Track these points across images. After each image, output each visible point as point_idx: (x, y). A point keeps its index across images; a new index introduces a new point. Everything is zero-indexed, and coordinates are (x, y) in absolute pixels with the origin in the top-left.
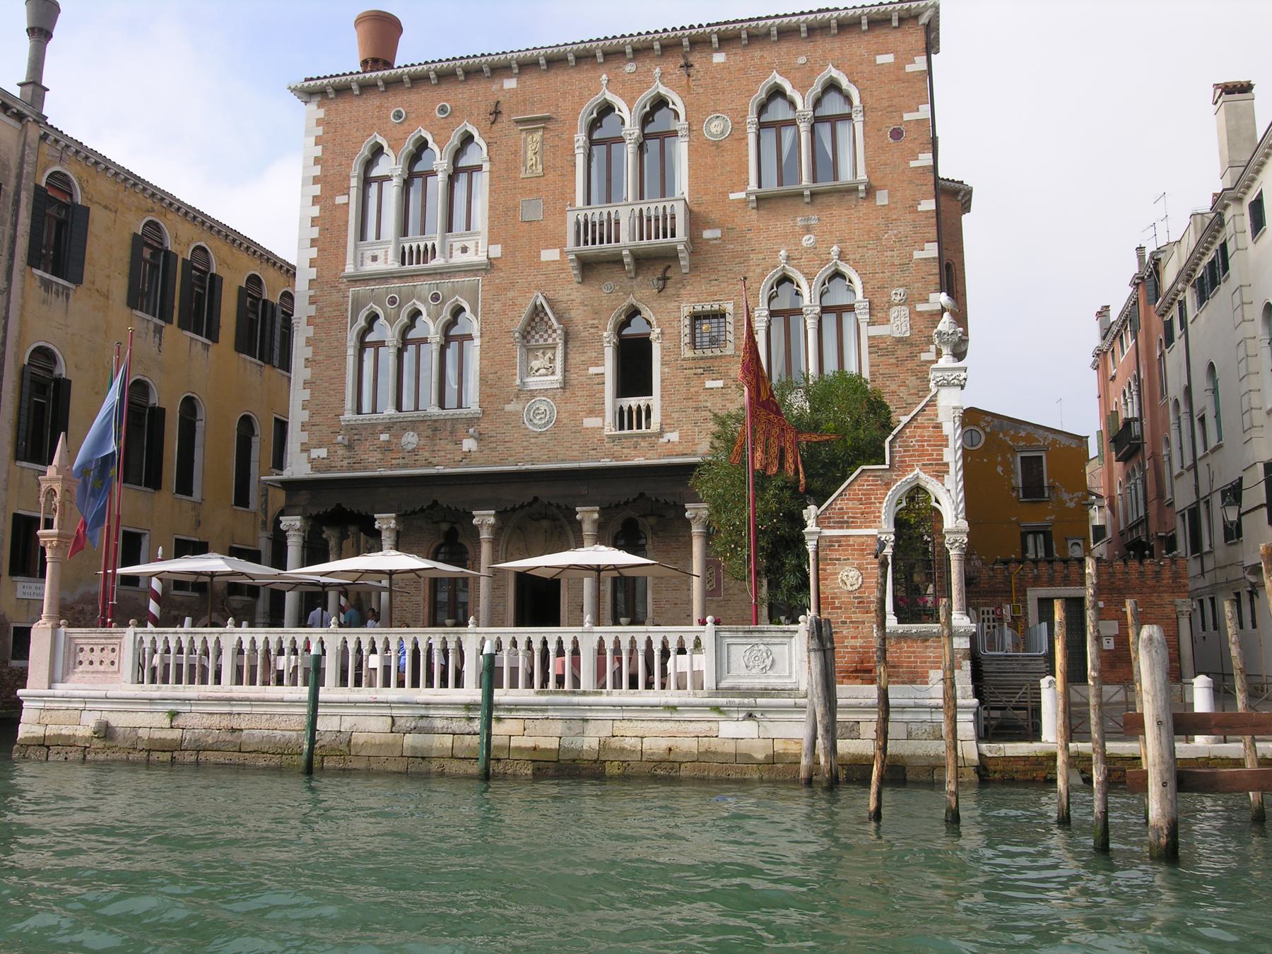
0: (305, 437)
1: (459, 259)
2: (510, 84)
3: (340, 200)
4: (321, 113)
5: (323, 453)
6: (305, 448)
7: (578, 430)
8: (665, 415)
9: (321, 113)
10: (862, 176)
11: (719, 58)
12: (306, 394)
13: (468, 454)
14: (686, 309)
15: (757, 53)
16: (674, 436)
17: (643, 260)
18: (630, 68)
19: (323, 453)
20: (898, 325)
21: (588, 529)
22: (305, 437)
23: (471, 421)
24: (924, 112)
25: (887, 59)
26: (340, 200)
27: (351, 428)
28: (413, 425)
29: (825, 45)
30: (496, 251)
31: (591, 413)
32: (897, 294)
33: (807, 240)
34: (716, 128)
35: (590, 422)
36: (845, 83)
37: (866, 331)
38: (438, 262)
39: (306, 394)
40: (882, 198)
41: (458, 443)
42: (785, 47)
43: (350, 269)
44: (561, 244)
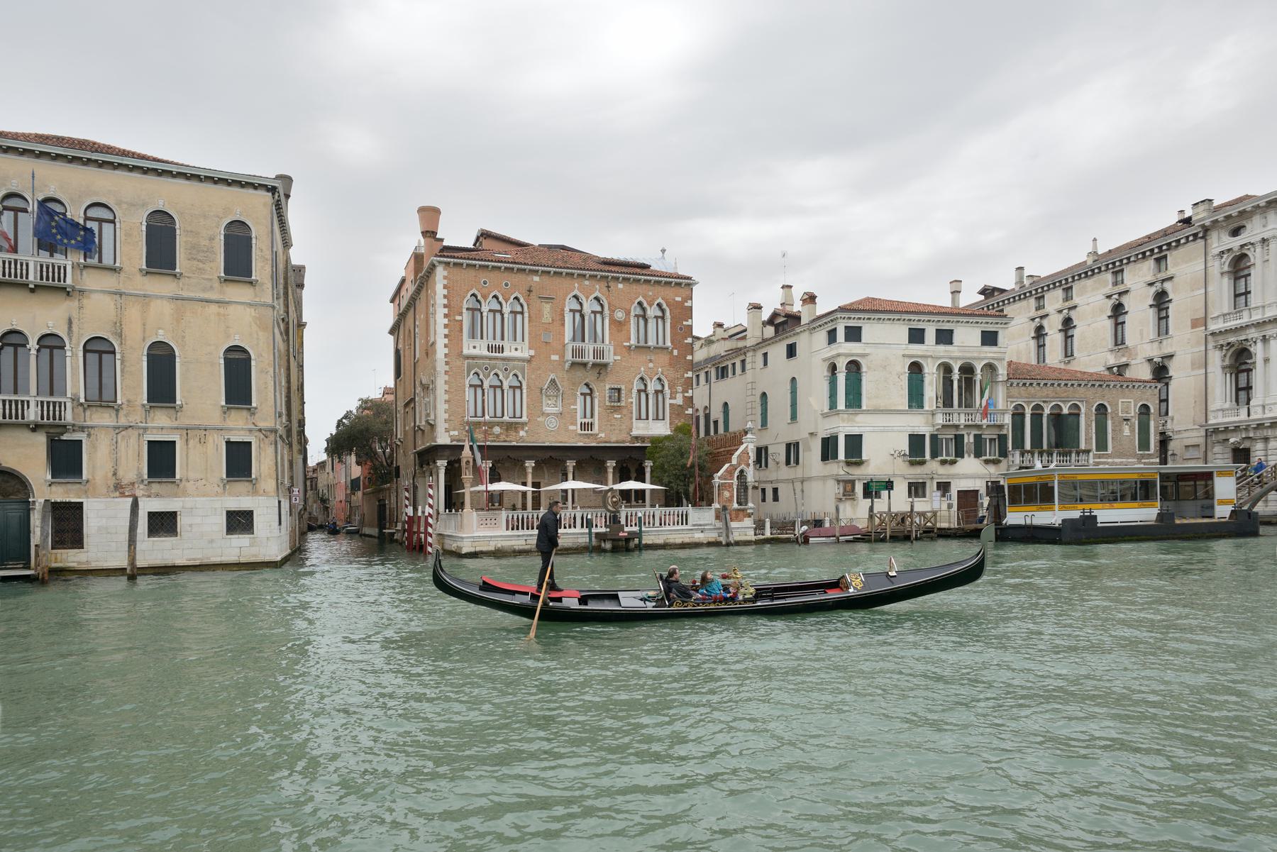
0: (447, 425)
1: (514, 354)
2: (536, 279)
3: (458, 318)
4: (445, 273)
5: (456, 433)
6: (447, 430)
7: (567, 430)
8: (600, 427)
9: (445, 273)
10: (669, 344)
11: (620, 286)
12: (446, 406)
13: (523, 437)
14: (608, 387)
15: (634, 287)
16: (603, 435)
17: (594, 365)
18: (587, 283)
19: (456, 433)
20: (679, 400)
21: (571, 469)
22: (447, 425)
23: (524, 424)
24: (689, 323)
25: (679, 299)
26: (458, 318)
27: (468, 423)
28: (498, 424)
29: (658, 288)
30: (532, 353)
31: (572, 424)
32: (680, 389)
33: (651, 365)
34: (620, 315)
35: (572, 428)
36: (664, 306)
37: (668, 402)
38: (506, 354)
39: (446, 406)
40: (675, 353)
41: (517, 432)
42: (645, 286)
43: (465, 352)
44: (562, 356)
